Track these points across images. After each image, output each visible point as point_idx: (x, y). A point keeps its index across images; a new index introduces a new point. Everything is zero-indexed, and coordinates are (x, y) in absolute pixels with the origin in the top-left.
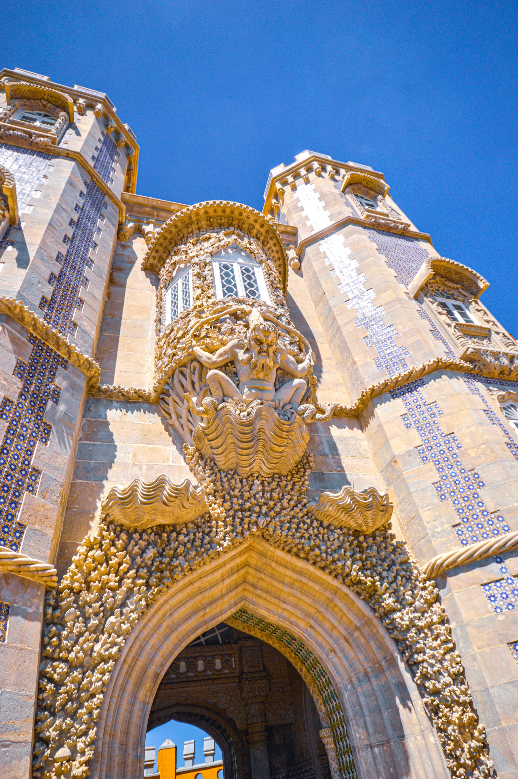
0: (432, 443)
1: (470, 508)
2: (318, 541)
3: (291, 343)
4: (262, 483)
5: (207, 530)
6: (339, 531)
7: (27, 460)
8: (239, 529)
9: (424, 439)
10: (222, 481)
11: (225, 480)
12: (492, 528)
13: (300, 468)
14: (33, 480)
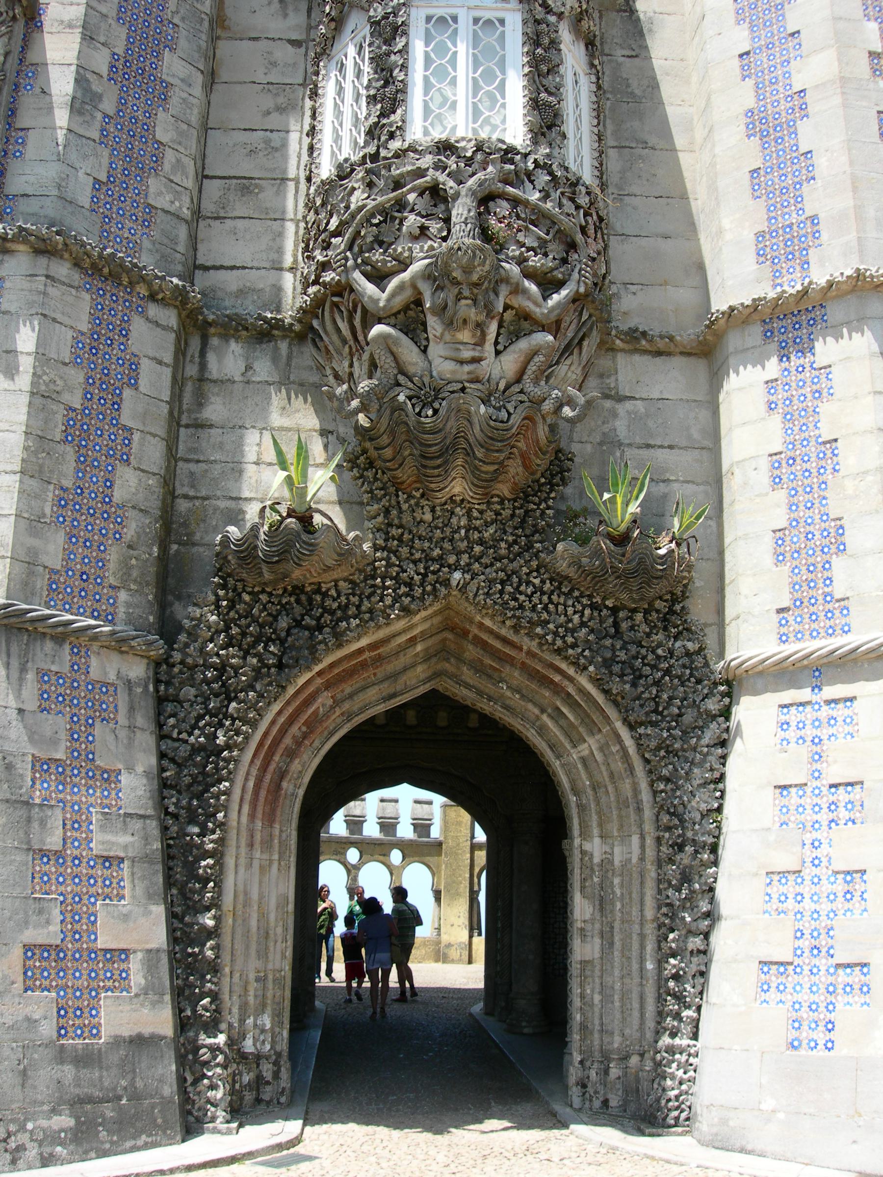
0: (798, 452)
1: (812, 584)
2: (545, 616)
3: (543, 243)
4: (469, 512)
5: (368, 591)
6: (585, 601)
7: (107, 496)
8: (418, 591)
9: (788, 439)
10: (400, 508)
11: (405, 507)
12: (828, 623)
13: (543, 484)
14: (119, 524)
